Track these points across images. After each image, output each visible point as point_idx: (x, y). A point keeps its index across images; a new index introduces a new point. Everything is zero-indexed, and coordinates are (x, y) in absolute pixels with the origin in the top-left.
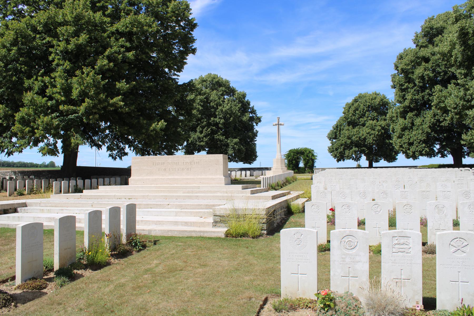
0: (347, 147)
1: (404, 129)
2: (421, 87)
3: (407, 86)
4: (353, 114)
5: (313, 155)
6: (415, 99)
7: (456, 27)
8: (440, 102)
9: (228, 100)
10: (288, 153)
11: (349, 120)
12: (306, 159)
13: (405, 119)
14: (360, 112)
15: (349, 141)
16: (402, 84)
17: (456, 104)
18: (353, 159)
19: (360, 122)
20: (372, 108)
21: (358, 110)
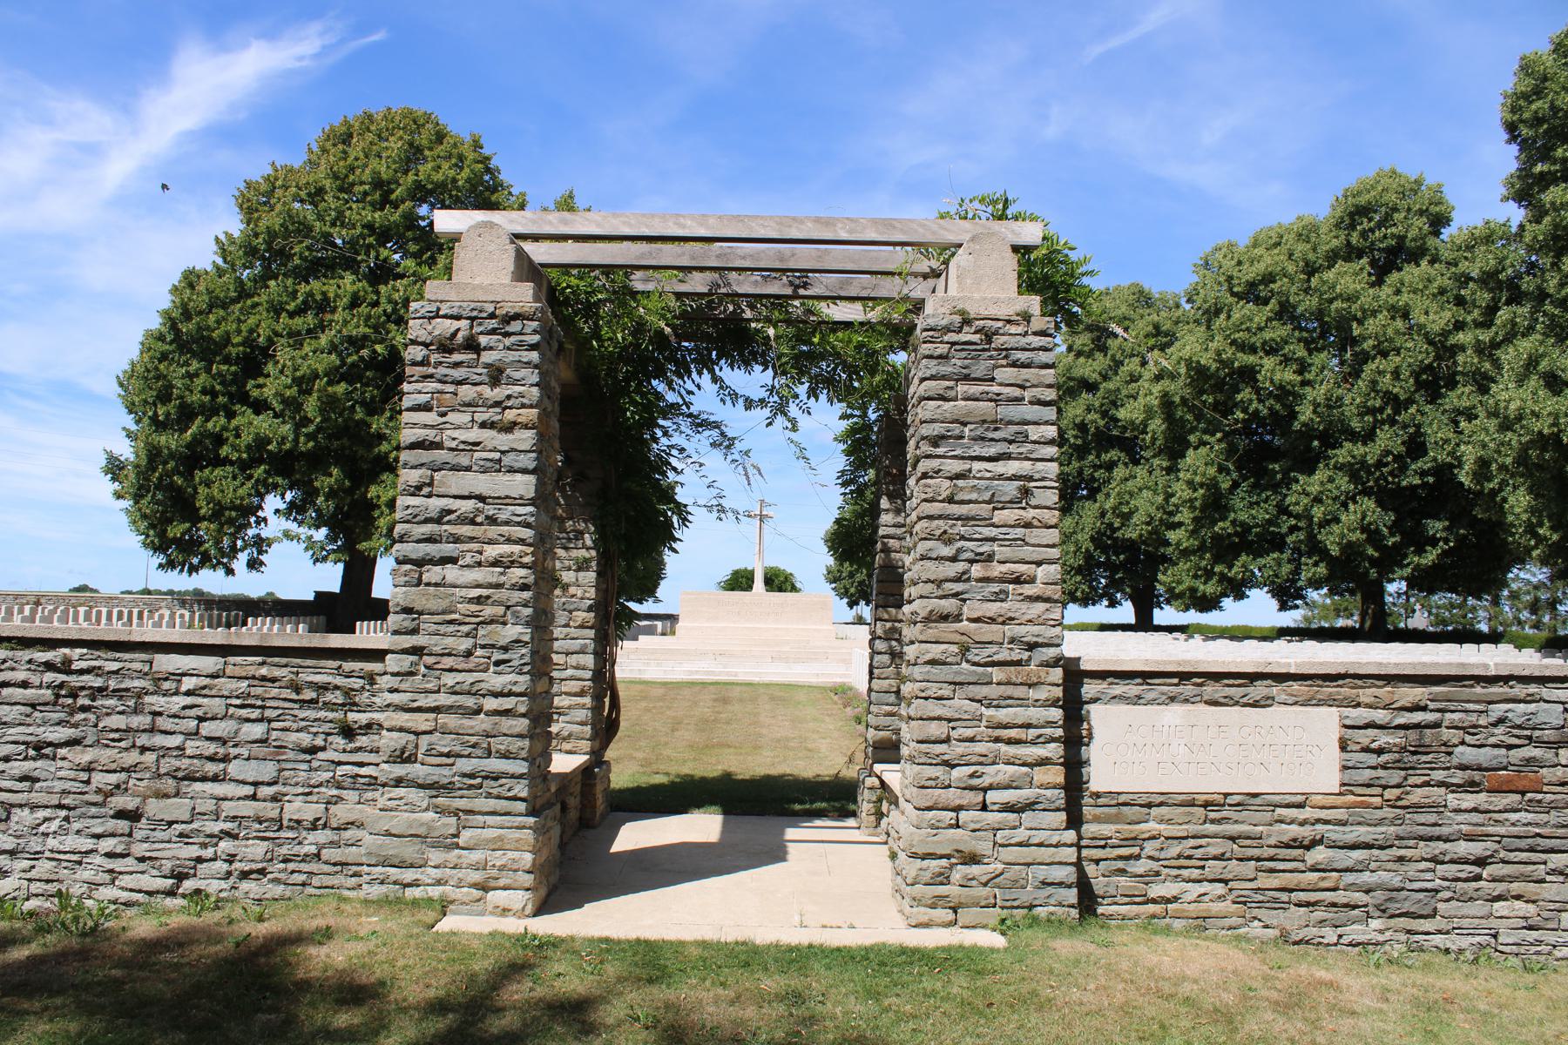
2: (1075, 448)
7: (1157, 389)
8: (1121, 503)
17: (1150, 516)
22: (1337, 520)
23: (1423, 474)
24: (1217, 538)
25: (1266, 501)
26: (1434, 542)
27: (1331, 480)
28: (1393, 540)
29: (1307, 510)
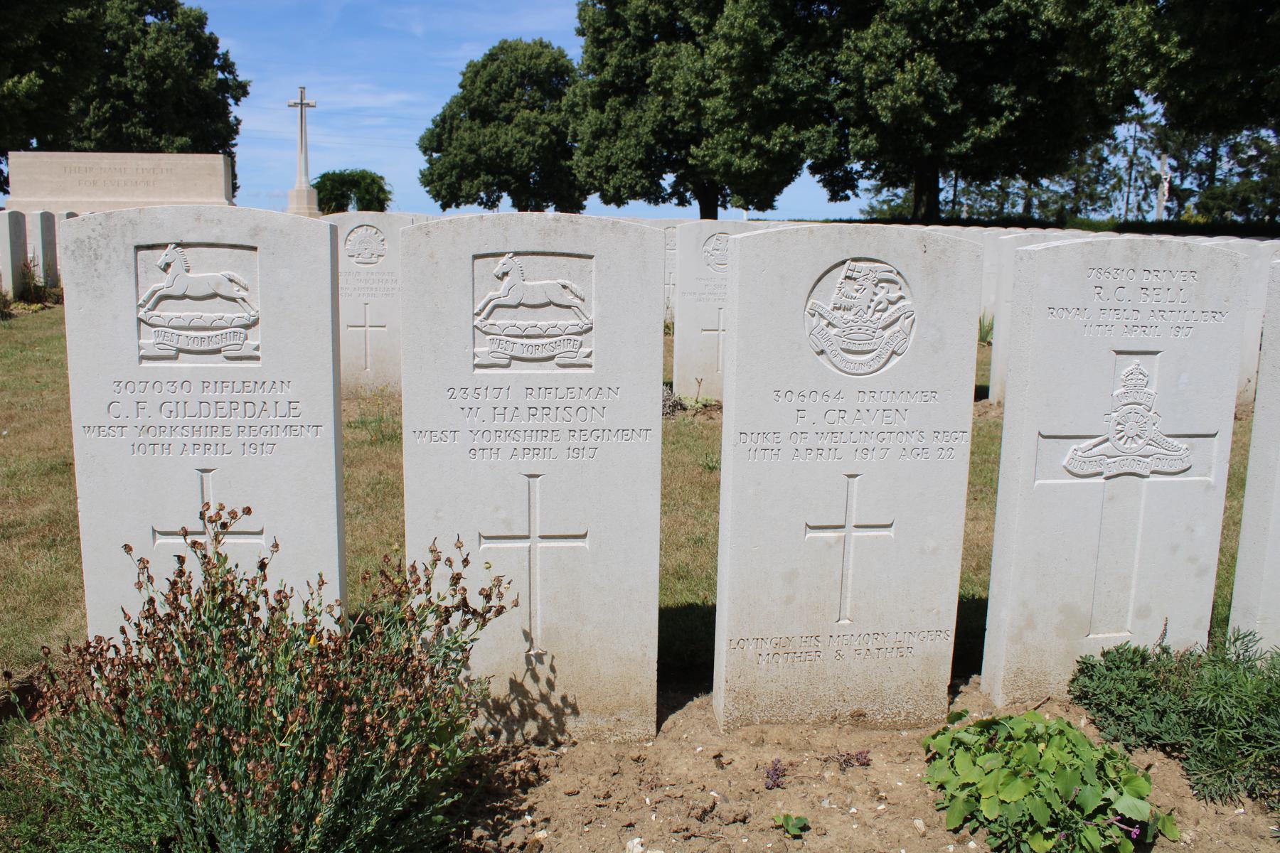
0: (467, 171)
1: (598, 134)
2: (639, 39)
3: (610, 34)
4: (483, 91)
5: (381, 189)
6: (626, 66)
9: (159, 31)
10: (318, 183)
11: (474, 104)
12: (364, 198)
13: (603, 111)
14: (502, 88)
15: (471, 159)
16: (599, 27)
17: (688, 84)
18: (480, 204)
19: (500, 112)
20: (528, 77)
21: (496, 82)
22: (891, 81)
23: (992, 27)
24: (757, 105)
25: (812, 63)
26: (998, 111)
27: (887, 34)
28: (954, 107)
29: (858, 69)
